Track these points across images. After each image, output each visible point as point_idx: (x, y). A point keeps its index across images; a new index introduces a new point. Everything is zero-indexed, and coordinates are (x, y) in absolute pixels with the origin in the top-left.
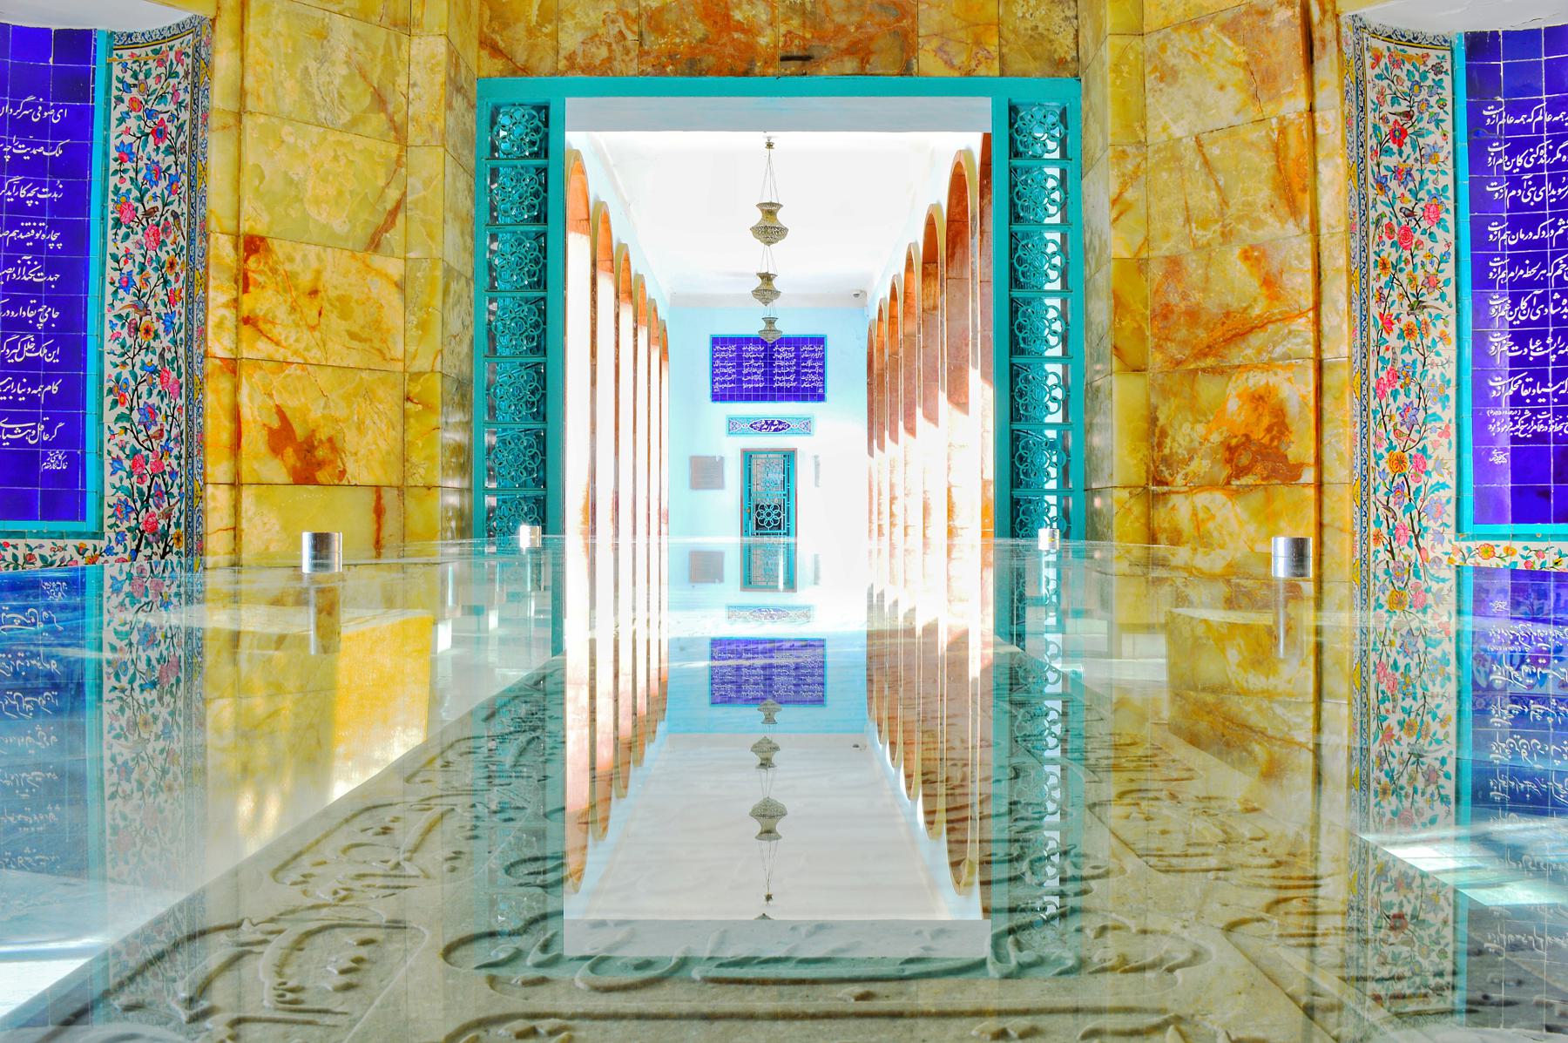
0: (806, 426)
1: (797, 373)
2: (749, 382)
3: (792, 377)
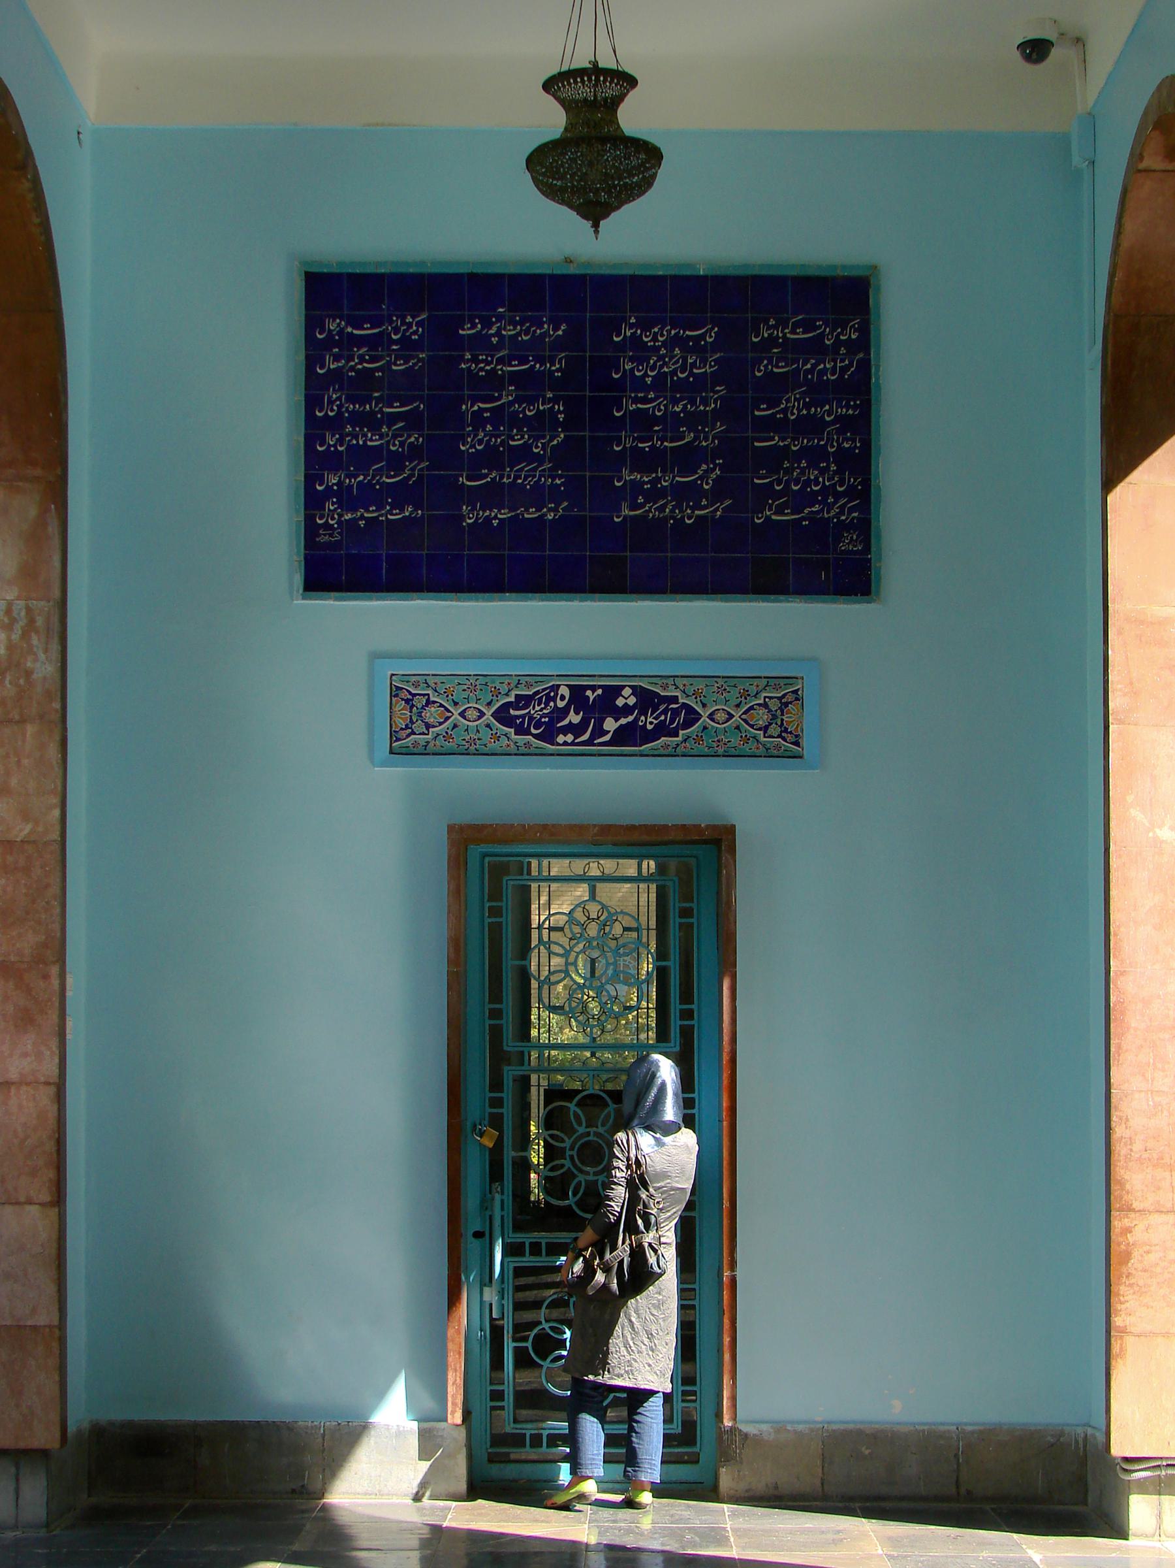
0: (773, 721)
2: (492, 495)
3: (708, 475)
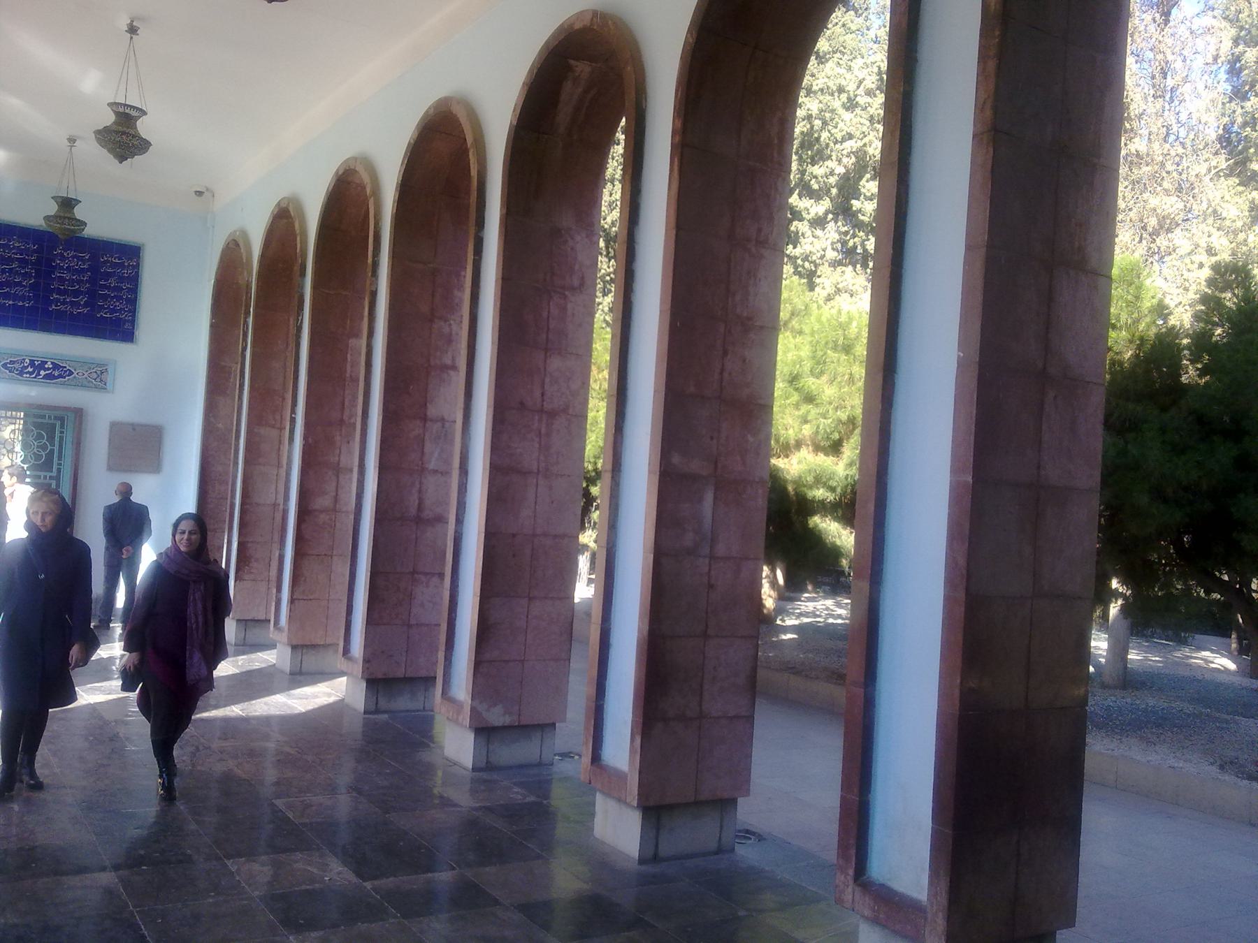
1: (92, 294)
3: (83, 300)
